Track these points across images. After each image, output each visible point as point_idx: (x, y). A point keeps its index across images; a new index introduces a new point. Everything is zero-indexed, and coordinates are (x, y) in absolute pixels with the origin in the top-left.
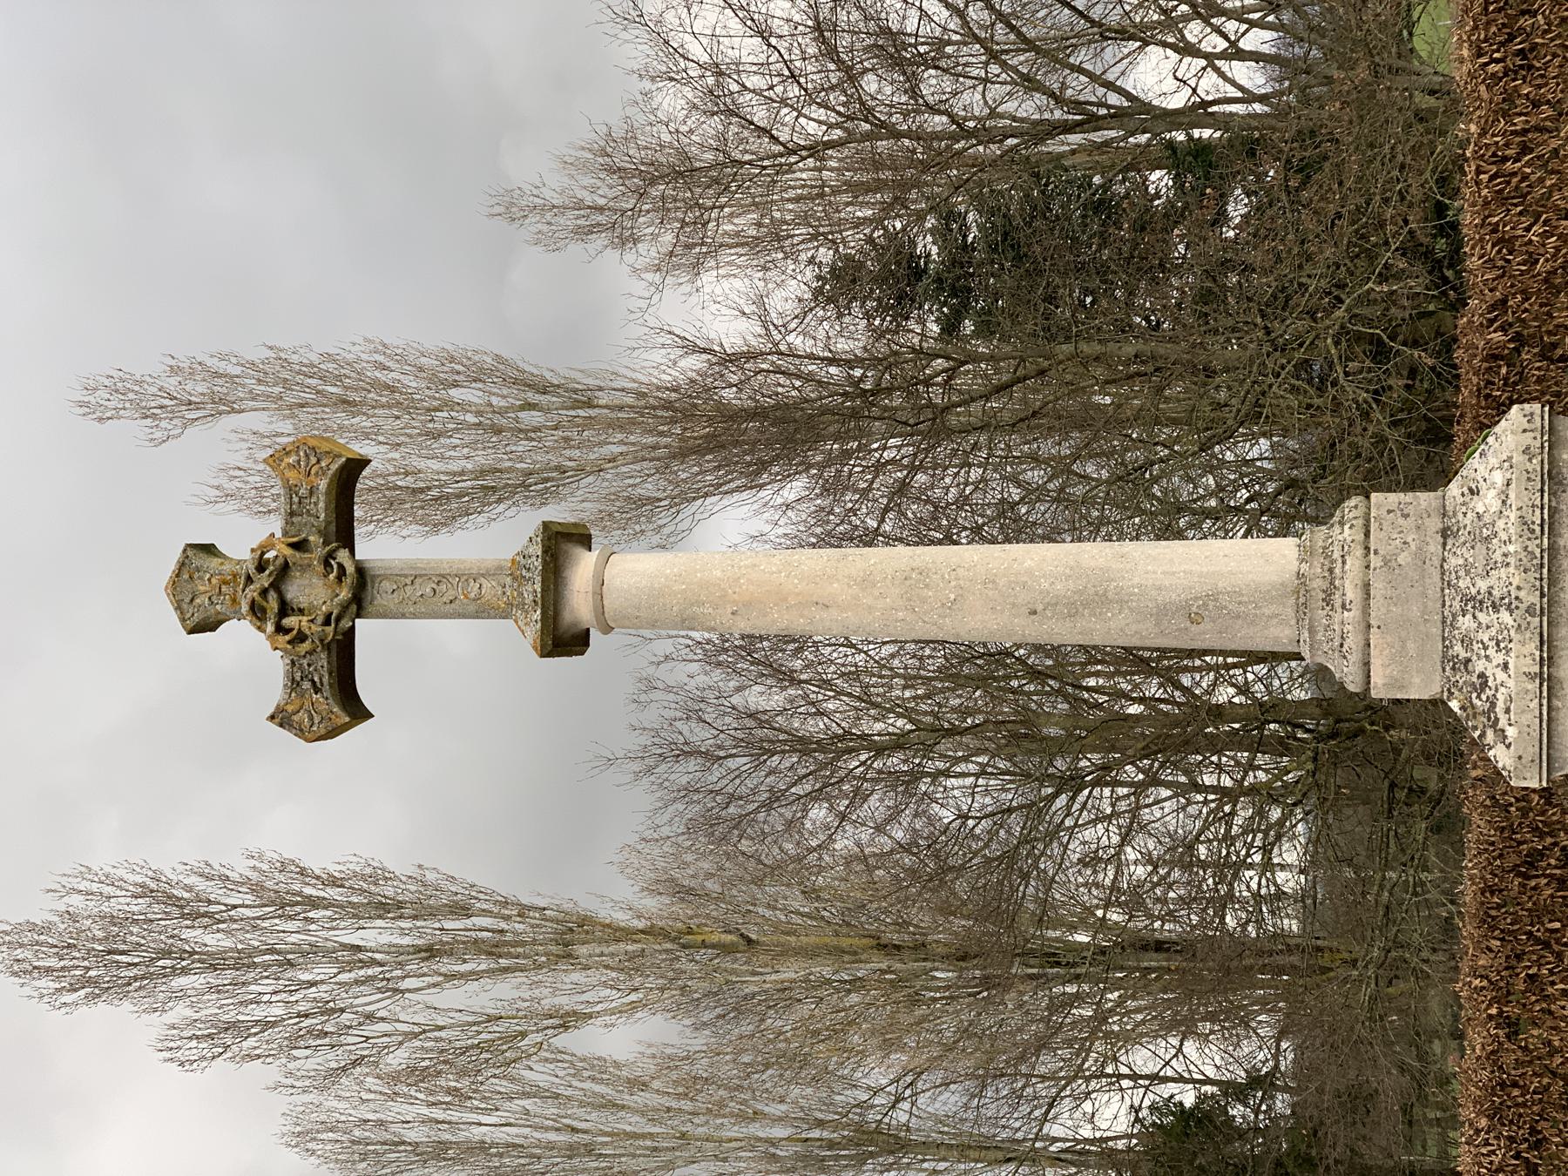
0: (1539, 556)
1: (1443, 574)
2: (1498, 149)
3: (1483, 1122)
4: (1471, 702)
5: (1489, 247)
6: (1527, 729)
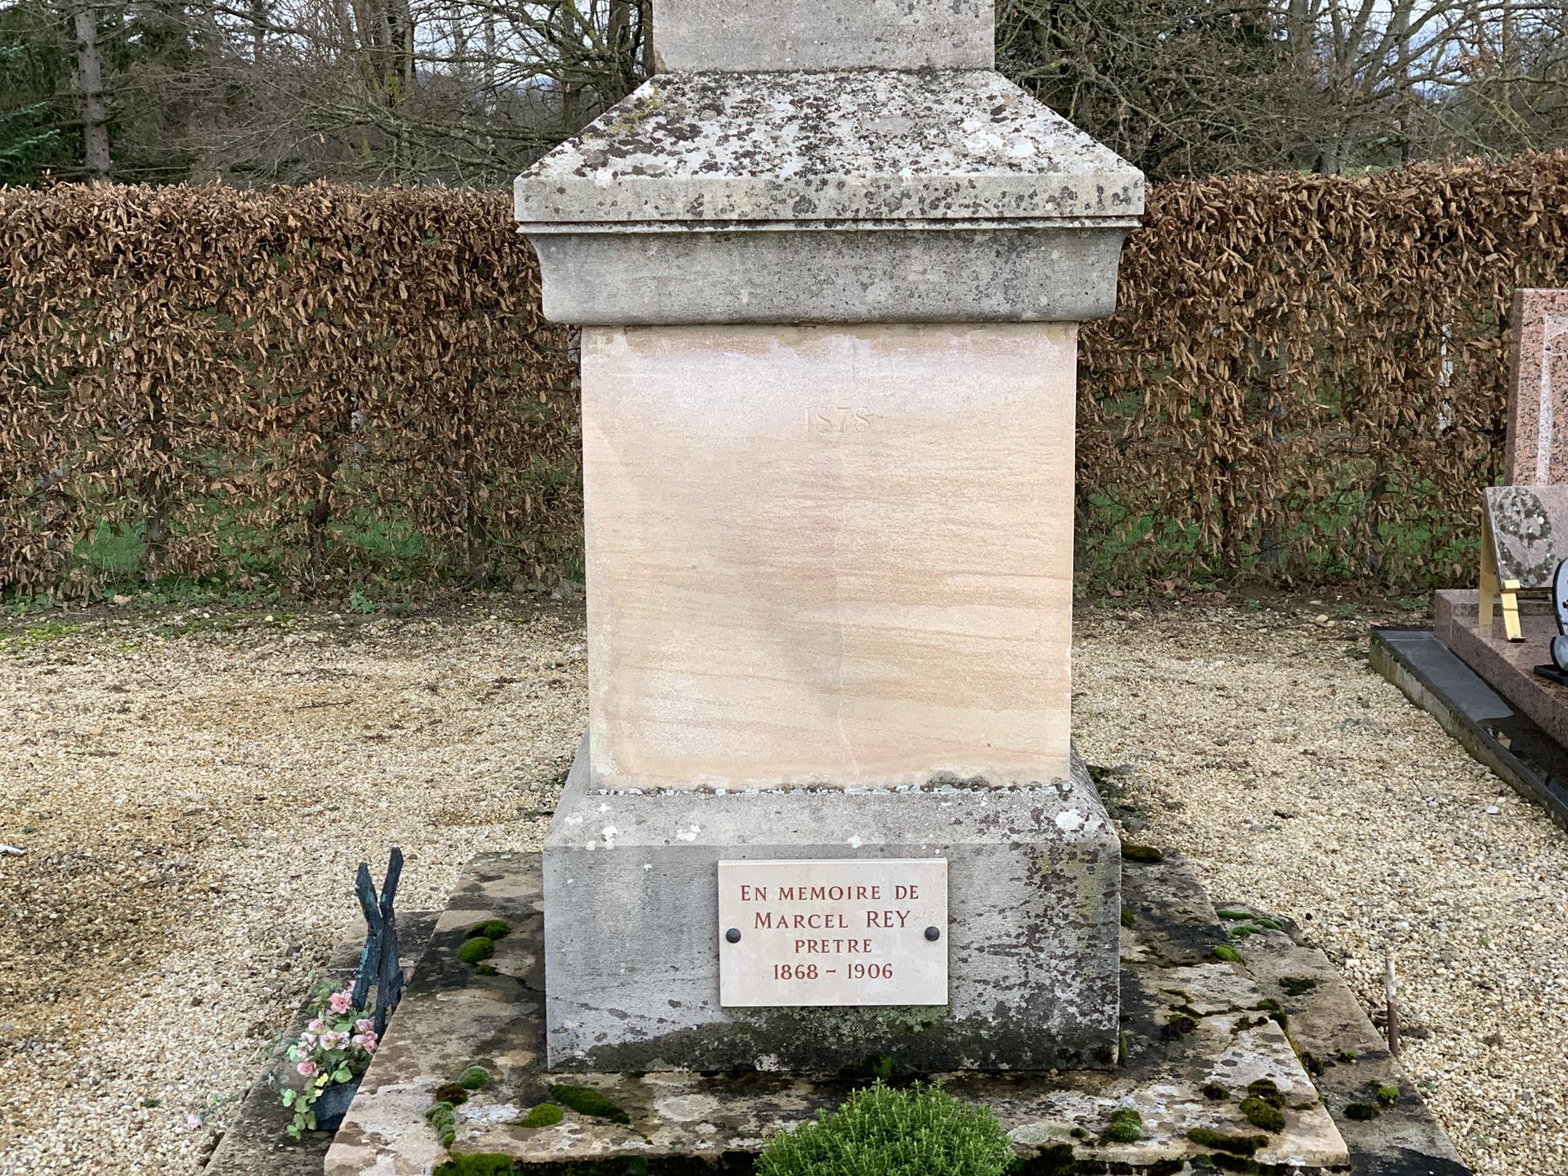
0: (895, 215)
1: (860, 70)
2: (1338, 212)
3: (155, 211)
4: (651, 115)
5: (1217, 204)
6: (609, 201)
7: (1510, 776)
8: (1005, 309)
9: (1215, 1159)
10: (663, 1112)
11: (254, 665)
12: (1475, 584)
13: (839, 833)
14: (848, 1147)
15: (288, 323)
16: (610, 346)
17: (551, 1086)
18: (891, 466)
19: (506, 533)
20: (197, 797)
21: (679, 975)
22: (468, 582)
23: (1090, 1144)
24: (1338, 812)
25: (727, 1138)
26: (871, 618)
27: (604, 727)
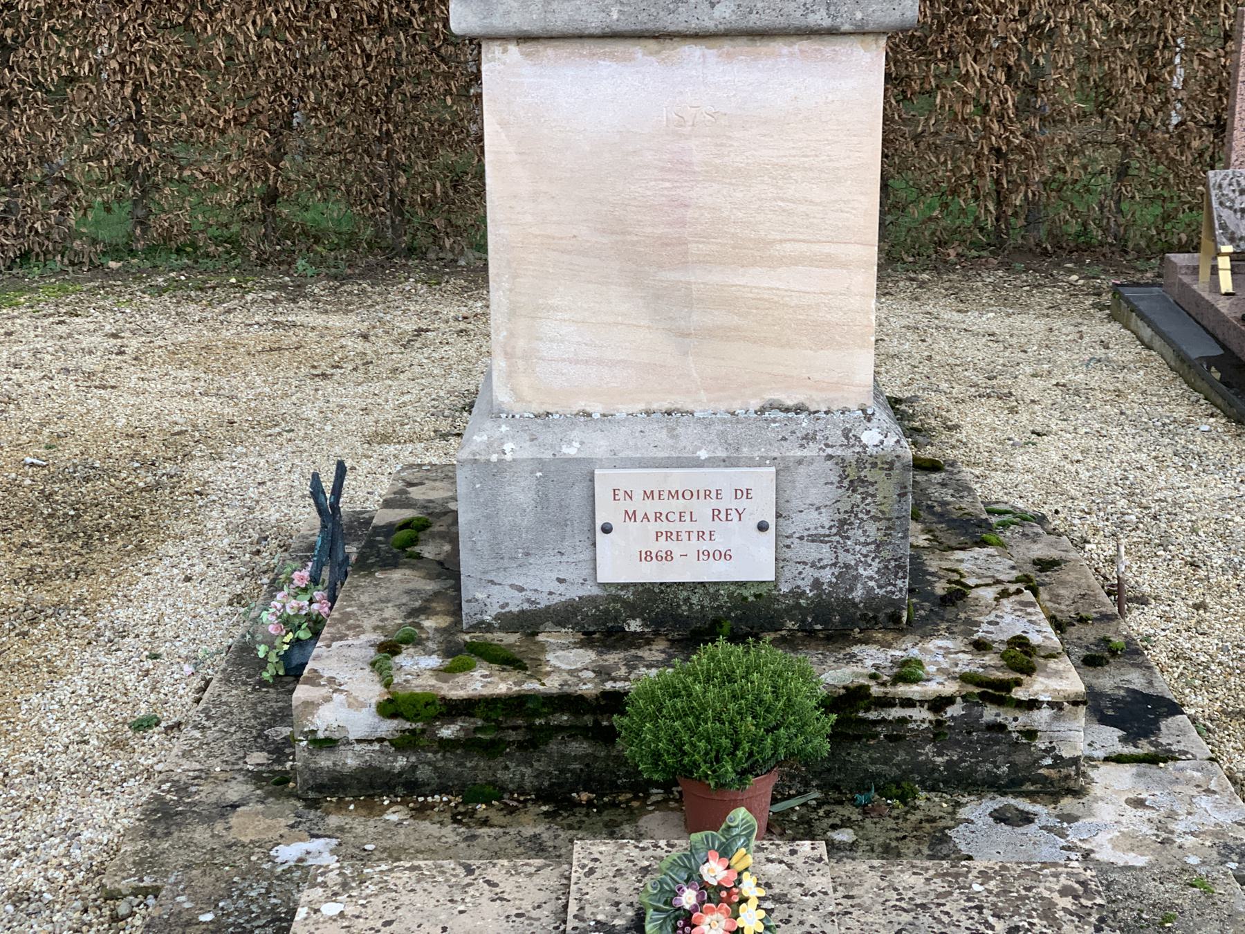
7: (1219, 401)
8: (827, 23)
9: (981, 695)
10: (553, 662)
11: (222, 318)
12: (1196, 249)
13: (690, 448)
14: (698, 687)
15: (241, 38)
16: (504, 56)
17: (466, 642)
18: (732, 155)
19: (421, 212)
20: (181, 421)
21: (564, 558)
22: (391, 252)
23: (884, 684)
24: (1082, 431)
25: (603, 681)
26: (715, 277)
27: (503, 364)
